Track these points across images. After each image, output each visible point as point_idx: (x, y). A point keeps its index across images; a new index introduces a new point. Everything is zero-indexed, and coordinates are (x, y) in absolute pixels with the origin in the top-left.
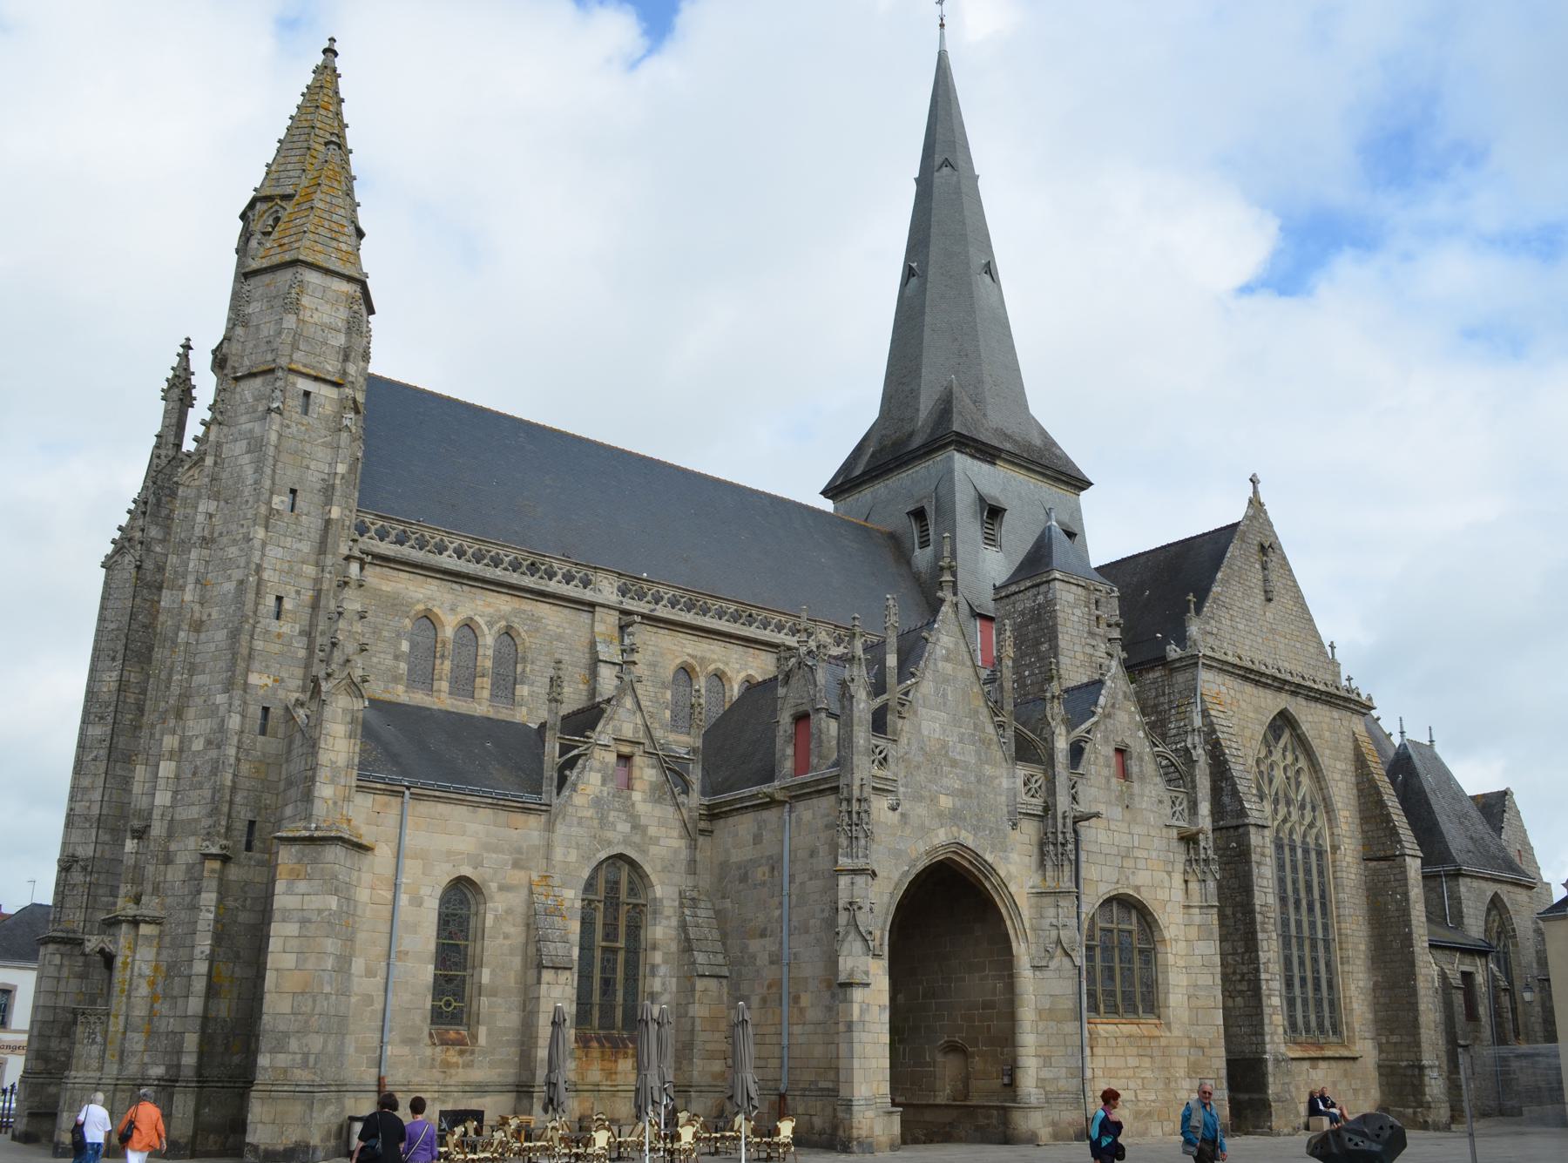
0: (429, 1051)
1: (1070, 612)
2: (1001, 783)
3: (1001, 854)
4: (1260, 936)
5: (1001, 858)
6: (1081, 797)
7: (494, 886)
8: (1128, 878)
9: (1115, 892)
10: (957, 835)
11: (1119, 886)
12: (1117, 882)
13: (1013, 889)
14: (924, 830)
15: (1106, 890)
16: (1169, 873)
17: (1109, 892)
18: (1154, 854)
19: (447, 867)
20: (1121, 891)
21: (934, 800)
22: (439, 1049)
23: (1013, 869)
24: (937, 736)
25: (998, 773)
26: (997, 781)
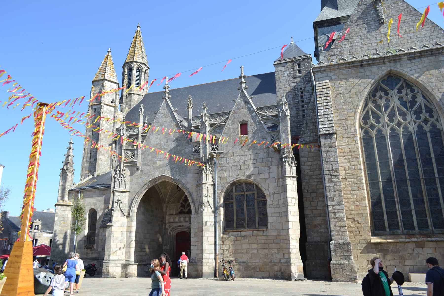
0: (84, 250)
1: (283, 74)
2: (185, 151)
3: (183, 175)
4: (327, 185)
5: (183, 177)
6: (219, 148)
7: (99, 209)
8: (244, 173)
9: (237, 179)
10: (163, 173)
11: (239, 177)
12: (238, 175)
13: (189, 186)
14: (150, 174)
15: (231, 180)
16: (269, 167)
17: (233, 180)
18: (259, 161)
19: (88, 207)
20: (239, 179)
21: (154, 163)
22: (86, 250)
23: (188, 179)
24: (157, 142)
25: (184, 148)
26: (183, 151)
